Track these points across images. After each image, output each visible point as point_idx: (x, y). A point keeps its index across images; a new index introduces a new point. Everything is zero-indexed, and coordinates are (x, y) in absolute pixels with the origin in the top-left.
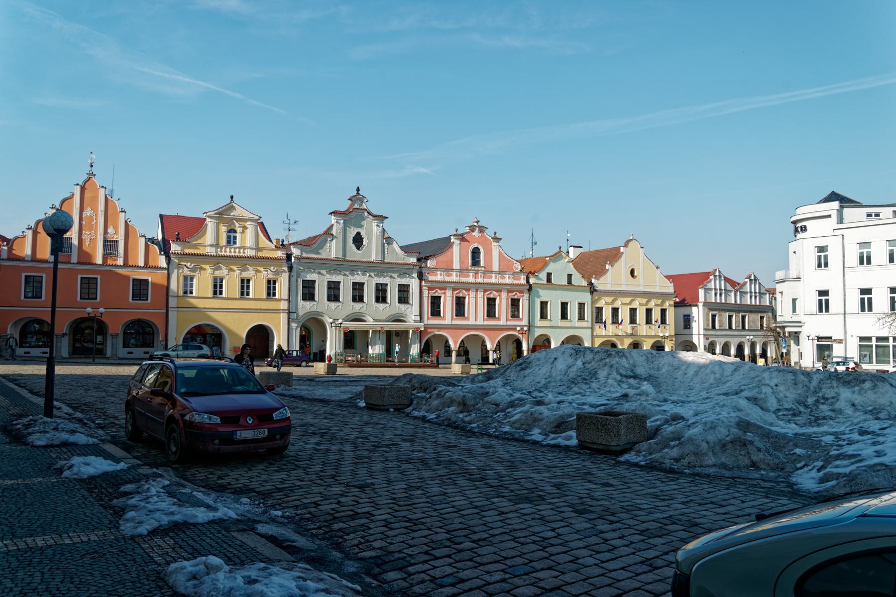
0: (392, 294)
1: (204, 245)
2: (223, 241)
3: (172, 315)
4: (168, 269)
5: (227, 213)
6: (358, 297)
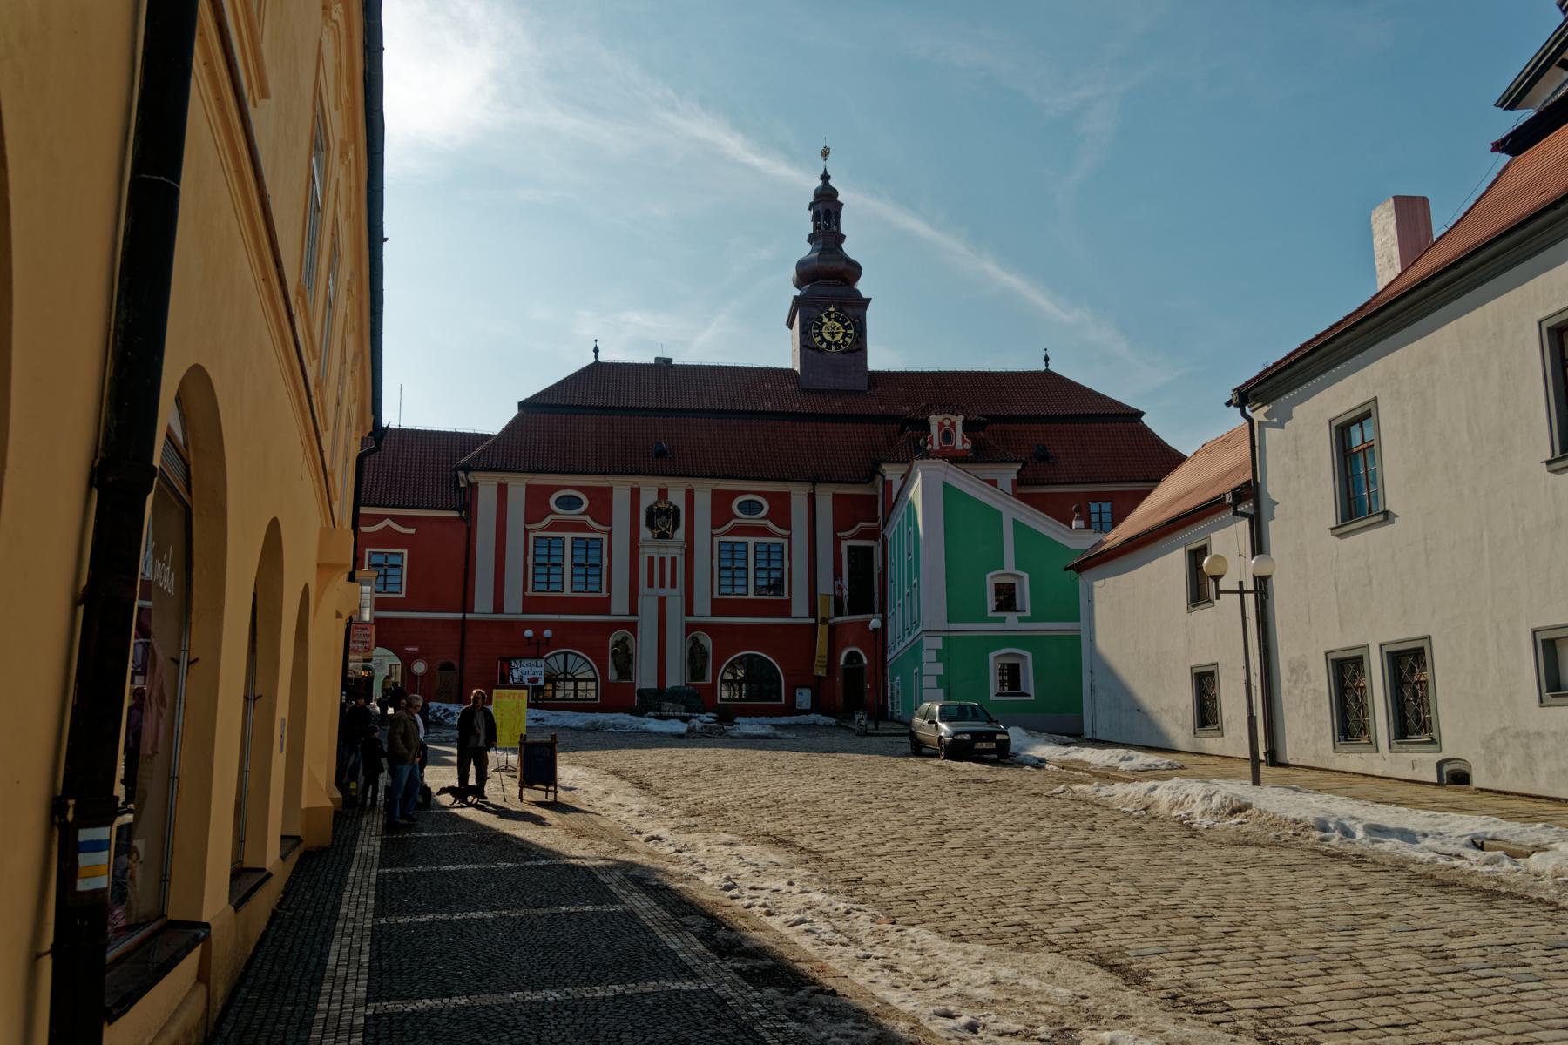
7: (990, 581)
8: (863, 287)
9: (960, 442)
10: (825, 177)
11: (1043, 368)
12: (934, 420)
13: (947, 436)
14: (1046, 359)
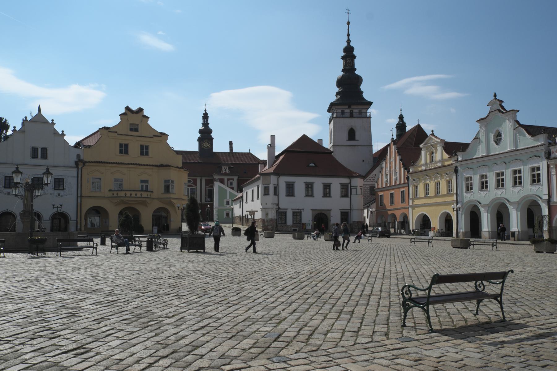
0: (526, 176)
1: (421, 166)
2: (428, 161)
3: (410, 209)
4: (408, 183)
5: (430, 142)
6: (500, 183)
7: (225, 200)
8: (213, 135)
9: (227, 171)
10: (205, 110)
11: (248, 152)
12: (223, 167)
13: (225, 170)
14: (249, 150)
